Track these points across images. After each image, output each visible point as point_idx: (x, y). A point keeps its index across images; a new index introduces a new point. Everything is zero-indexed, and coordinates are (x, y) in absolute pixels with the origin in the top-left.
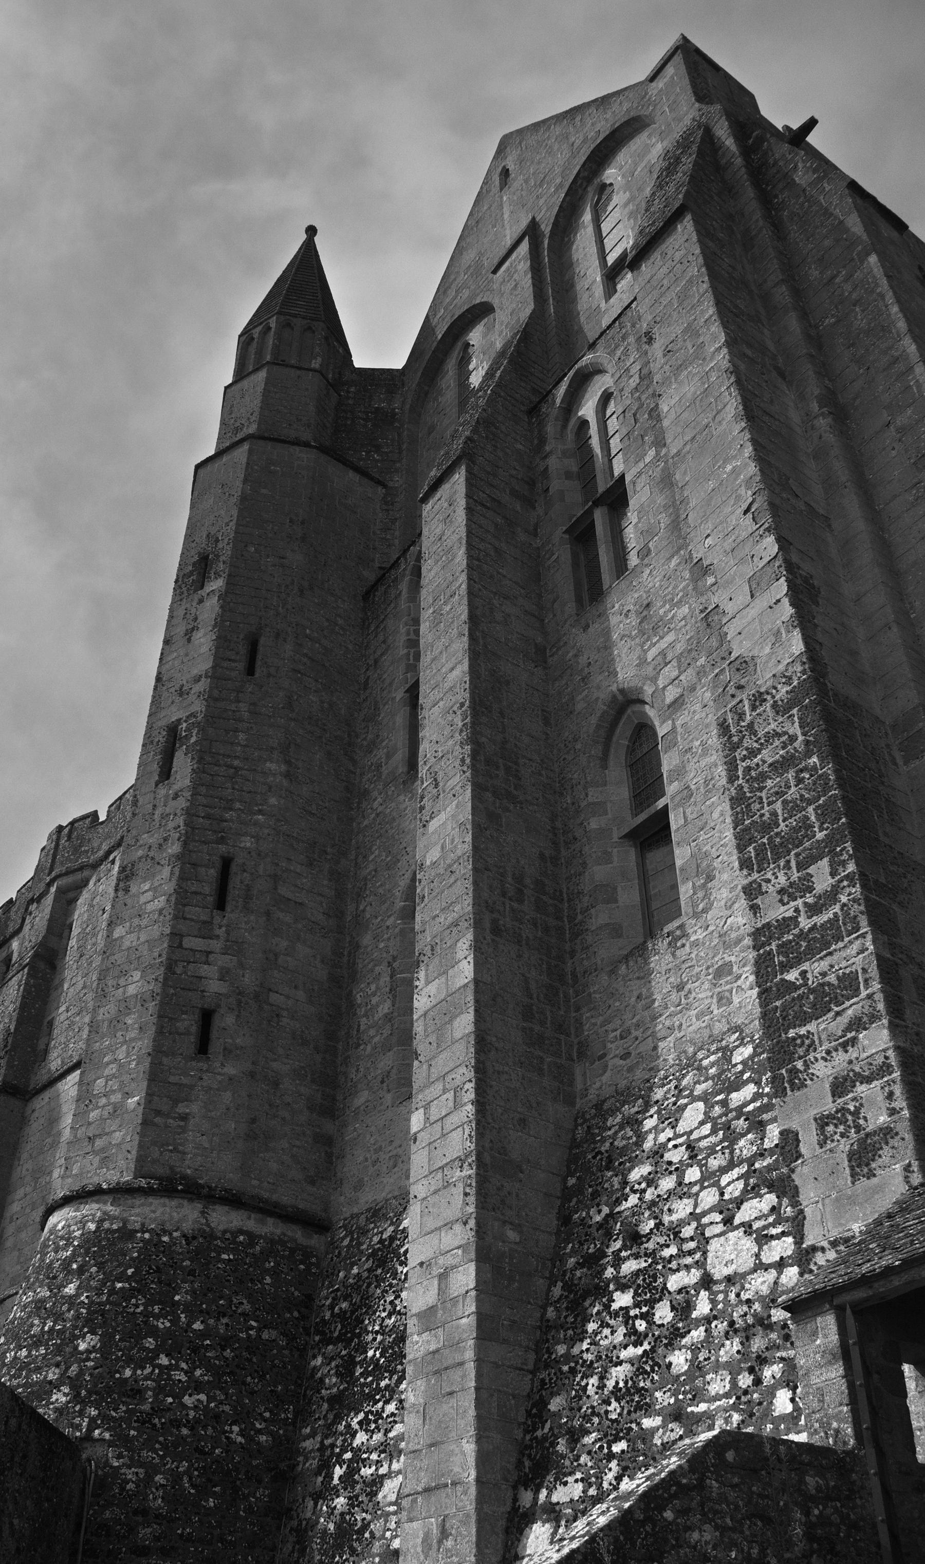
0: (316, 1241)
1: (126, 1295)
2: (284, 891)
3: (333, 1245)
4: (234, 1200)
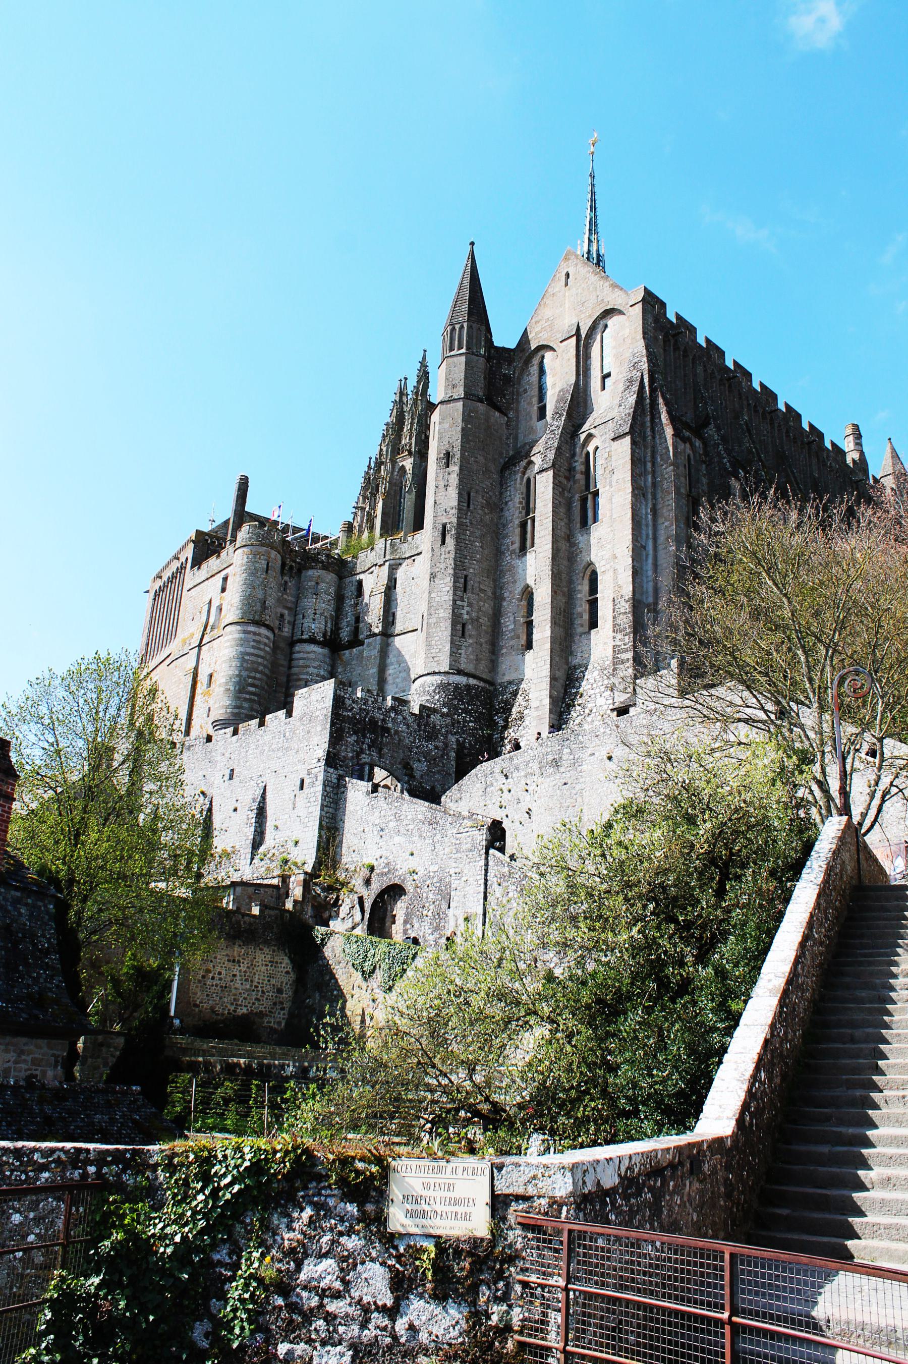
0: (491, 688)
1: (452, 699)
2: (482, 587)
3: (496, 690)
4: (474, 677)
